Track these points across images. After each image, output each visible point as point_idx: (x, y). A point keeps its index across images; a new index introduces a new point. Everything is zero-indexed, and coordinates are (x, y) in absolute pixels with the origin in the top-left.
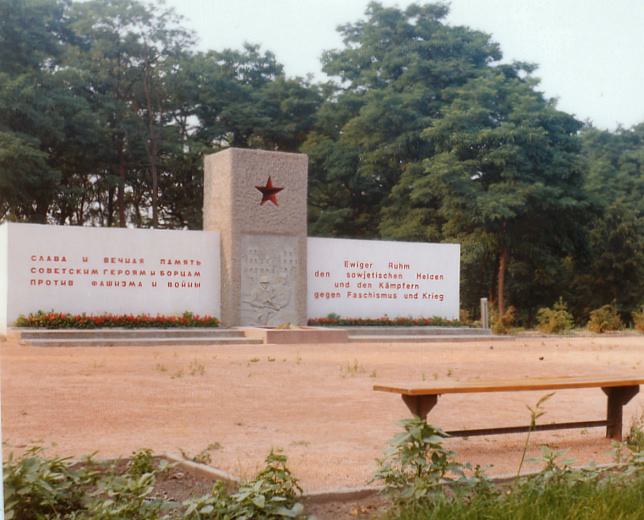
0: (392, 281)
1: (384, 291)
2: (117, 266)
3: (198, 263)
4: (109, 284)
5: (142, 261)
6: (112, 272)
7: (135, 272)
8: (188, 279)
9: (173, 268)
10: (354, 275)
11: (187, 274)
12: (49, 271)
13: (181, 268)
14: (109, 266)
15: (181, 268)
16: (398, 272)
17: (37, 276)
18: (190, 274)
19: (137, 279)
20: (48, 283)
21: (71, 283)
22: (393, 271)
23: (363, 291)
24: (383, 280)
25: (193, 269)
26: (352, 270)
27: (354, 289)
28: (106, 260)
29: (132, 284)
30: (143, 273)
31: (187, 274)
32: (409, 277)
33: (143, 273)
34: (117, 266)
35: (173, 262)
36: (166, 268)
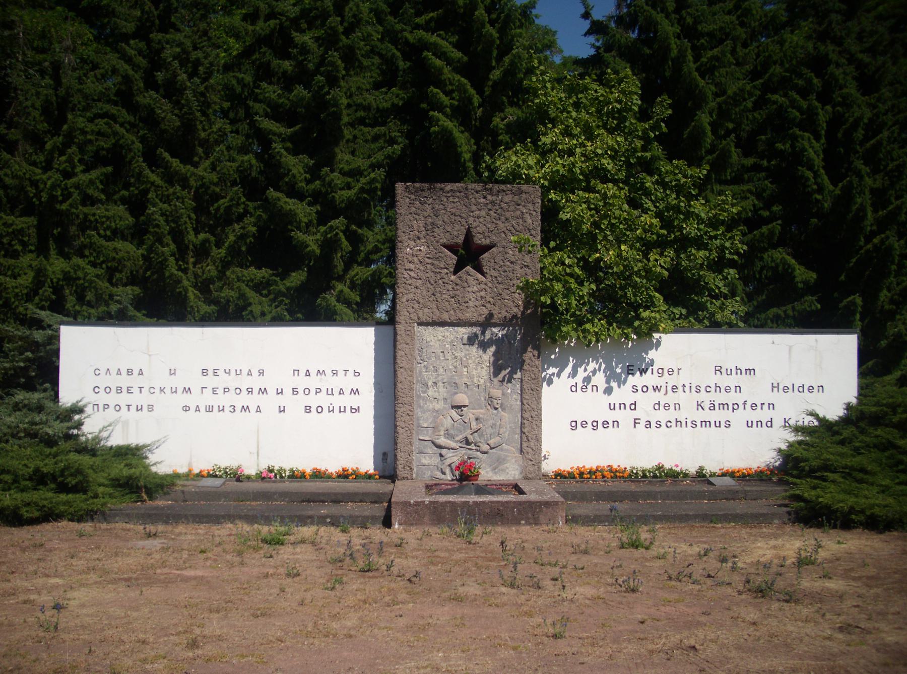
0: (721, 398)
2: (223, 380)
3: (357, 374)
4: (210, 409)
5: (261, 373)
6: (214, 391)
8: (338, 401)
9: (314, 382)
11: (336, 392)
12: (119, 390)
14: (210, 381)
16: (732, 380)
18: (341, 392)
19: (252, 401)
20: (118, 408)
21: (151, 408)
22: (724, 381)
23: (662, 416)
27: (645, 411)
28: (205, 372)
29: (245, 409)
30: (263, 391)
31: (336, 392)
33: (263, 391)
34: (223, 380)
35: (313, 372)
36: (301, 382)
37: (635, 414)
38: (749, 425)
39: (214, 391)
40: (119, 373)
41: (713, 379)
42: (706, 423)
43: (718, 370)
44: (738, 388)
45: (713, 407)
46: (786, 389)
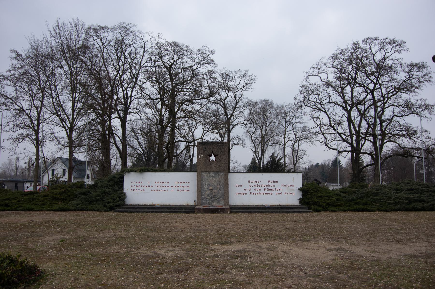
1: (267, 192)
3: (189, 183)
4: (157, 190)
5: (168, 182)
6: (158, 186)
7: (166, 186)
8: (185, 189)
9: (179, 185)
10: (252, 186)
13: (182, 185)
14: (157, 184)
15: (182, 185)
16: (273, 184)
17: (133, 188)
19: (166, 189)
20: (137, 190)
21: (144, 190)
22: (270, 184)
23: (257, 192)
24: (266, 187)
25: (187, 185)
26: (251, 184)
27: (252, 191)
28: (156, 182)
29: (165, 190)
30: (168, 187)
32: (278, 186)
33: (168, 187)
37: (251, 191)
38: (277, 194)
39: (158, 186)
40: (137, 182)
41: (268, 184)
42: (266, 193)
43: (269, 181)
44: (274, 186)
45: (268, 190)
46: (285, 186)
